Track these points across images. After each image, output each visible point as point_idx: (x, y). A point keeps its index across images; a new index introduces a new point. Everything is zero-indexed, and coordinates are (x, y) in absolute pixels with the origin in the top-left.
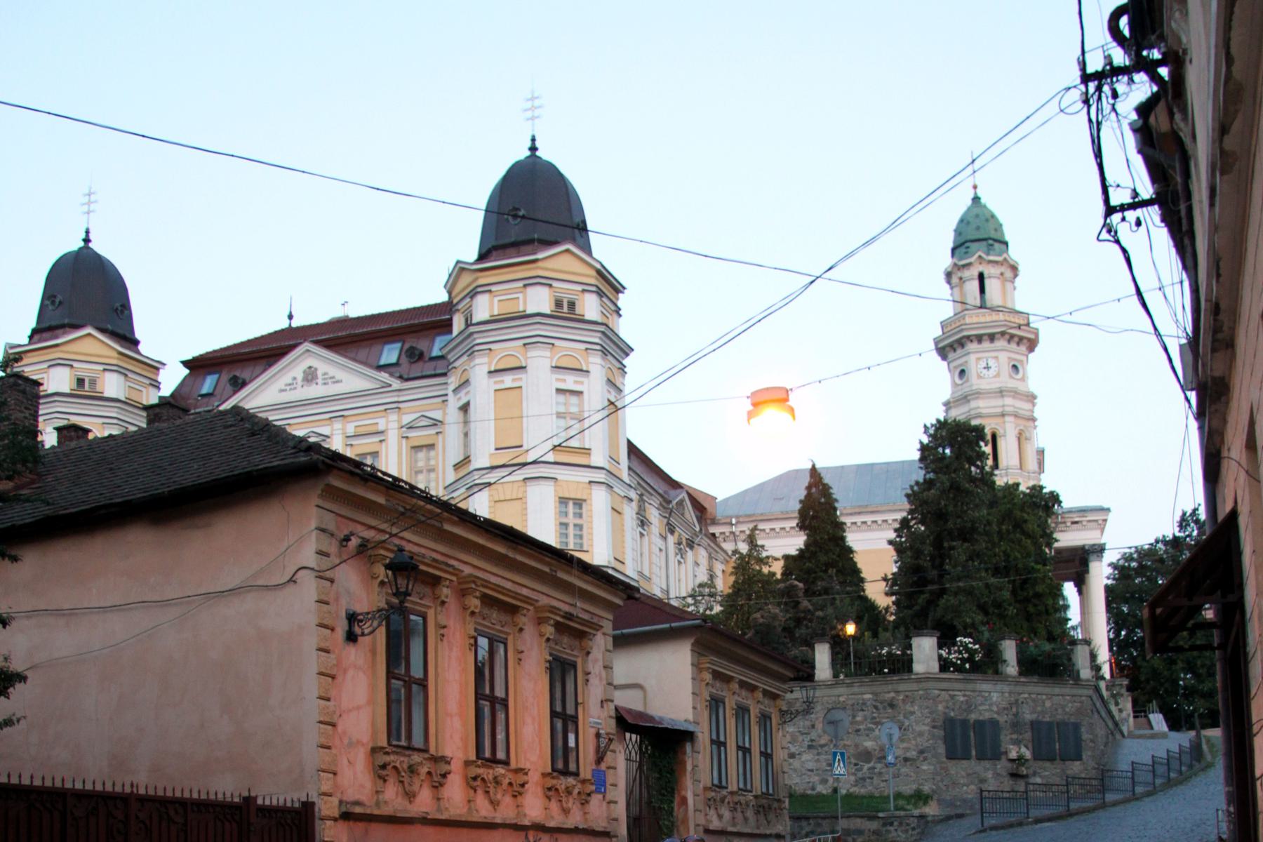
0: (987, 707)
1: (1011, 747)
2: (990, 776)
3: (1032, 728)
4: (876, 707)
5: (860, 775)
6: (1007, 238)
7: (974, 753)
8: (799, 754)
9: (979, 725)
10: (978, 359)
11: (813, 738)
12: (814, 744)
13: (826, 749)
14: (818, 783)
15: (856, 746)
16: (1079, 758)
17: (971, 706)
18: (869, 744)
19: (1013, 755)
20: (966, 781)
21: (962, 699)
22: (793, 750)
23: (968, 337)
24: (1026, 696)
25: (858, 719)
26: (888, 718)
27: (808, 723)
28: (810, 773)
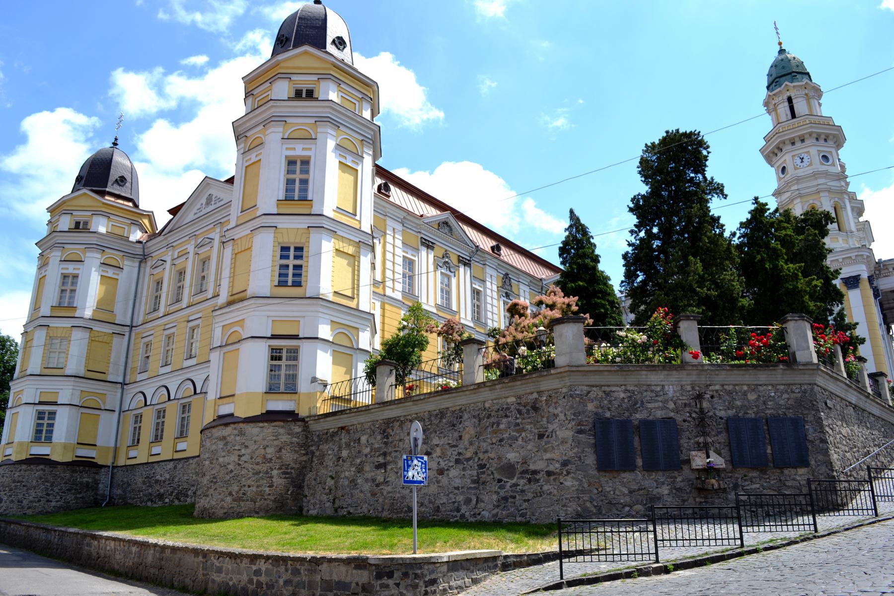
0: (660, 404)
1: (693, 453)
2: (666, 492)
3: (727, 429)
4: (519, 412)
5: (502, 493)
6: (808, 70)
7: (639, 462)
8: (447, 470)
9: (648, 426)
10: (793, 156)
11: (460, 451)
12: (461, 457)
13: (471, 463)
14: (462, 503)
15: (500, 458)
16: (805, 463)
17: (636, 404)
18: (512, 456)
19: (699, 461)
20: (628, 499)
21: (622, 395)
22: (443, 464)
23: (784, 142)
24: (717, 387)
25: (502, 426)
26: (531, 423)
27: (456, 435)
28: (457, 491)
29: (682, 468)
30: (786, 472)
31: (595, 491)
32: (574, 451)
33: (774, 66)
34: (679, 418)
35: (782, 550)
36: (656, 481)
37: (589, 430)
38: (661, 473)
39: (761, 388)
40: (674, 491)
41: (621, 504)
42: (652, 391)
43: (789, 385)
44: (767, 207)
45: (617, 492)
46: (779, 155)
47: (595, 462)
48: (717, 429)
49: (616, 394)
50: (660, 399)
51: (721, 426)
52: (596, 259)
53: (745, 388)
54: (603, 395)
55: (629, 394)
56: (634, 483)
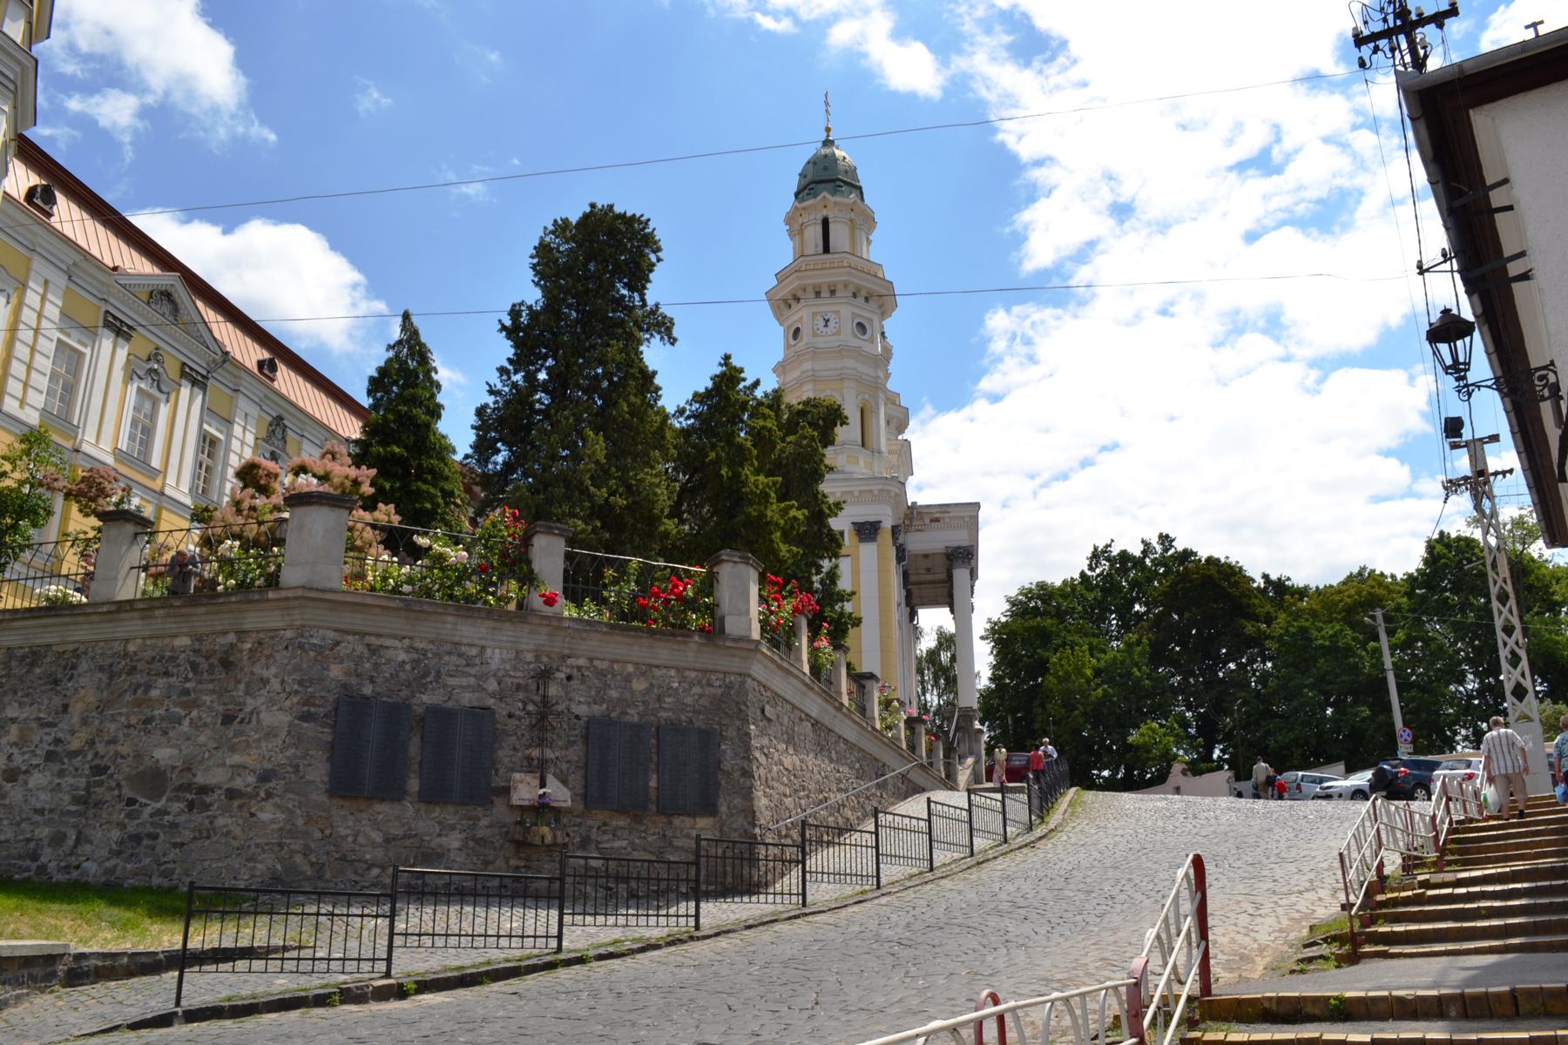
0: (472, 681)
1: (517, 776)
2: (456, 844)
3: (586, 738)
4: (194, 666)
5: (132, 827)
6: (862, 184)
7: (414, 784)
8: (27, 772)
9: (441, 717)
11: (60, 735)
12: (59, 749)
13: (77, 761)
14: (46, 842)
15: (138, 756)
16: (709, 808)
18: (164, 754)
19: (525, 791)
20: (379, 853)
21: (402, 656)
22: (18, 760)
24: (581, 662)
25: (155, 693)
26: (214, 691)
27: (57, 701)
28: (38, 818)
29: (492, 802)
30: (677, 821)
31: (318, 835)
32: (288, 753)
33: (813, 162)
34: (501, 711)
35: (628, 960)
36: (440, 823)
37: (325, 716)
38: (451, 809)
39: (657, 672)
40: (471, 844)
41: (366, 862)
42: (460, 655)
43: (706, 671)
44: (743, 375)
45: (361, 839)
46: (793, 306)
47: (326, 779)
48: (568, 736)
49: (390, 653)
50: (473, 671)
51: (576, 732)
52: (435, 412)
53: (630, 668)
54: (366, 651)
55: (415, 656)
56: (397, 823)
